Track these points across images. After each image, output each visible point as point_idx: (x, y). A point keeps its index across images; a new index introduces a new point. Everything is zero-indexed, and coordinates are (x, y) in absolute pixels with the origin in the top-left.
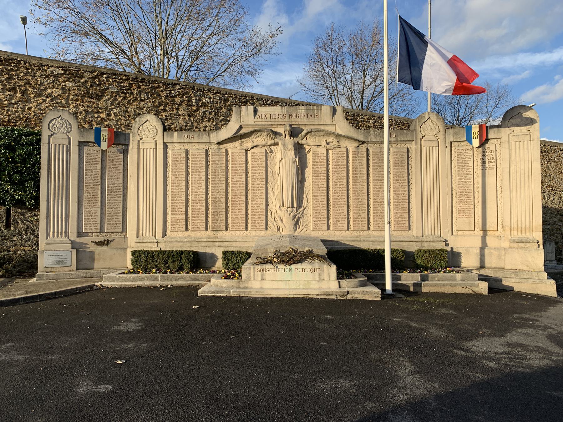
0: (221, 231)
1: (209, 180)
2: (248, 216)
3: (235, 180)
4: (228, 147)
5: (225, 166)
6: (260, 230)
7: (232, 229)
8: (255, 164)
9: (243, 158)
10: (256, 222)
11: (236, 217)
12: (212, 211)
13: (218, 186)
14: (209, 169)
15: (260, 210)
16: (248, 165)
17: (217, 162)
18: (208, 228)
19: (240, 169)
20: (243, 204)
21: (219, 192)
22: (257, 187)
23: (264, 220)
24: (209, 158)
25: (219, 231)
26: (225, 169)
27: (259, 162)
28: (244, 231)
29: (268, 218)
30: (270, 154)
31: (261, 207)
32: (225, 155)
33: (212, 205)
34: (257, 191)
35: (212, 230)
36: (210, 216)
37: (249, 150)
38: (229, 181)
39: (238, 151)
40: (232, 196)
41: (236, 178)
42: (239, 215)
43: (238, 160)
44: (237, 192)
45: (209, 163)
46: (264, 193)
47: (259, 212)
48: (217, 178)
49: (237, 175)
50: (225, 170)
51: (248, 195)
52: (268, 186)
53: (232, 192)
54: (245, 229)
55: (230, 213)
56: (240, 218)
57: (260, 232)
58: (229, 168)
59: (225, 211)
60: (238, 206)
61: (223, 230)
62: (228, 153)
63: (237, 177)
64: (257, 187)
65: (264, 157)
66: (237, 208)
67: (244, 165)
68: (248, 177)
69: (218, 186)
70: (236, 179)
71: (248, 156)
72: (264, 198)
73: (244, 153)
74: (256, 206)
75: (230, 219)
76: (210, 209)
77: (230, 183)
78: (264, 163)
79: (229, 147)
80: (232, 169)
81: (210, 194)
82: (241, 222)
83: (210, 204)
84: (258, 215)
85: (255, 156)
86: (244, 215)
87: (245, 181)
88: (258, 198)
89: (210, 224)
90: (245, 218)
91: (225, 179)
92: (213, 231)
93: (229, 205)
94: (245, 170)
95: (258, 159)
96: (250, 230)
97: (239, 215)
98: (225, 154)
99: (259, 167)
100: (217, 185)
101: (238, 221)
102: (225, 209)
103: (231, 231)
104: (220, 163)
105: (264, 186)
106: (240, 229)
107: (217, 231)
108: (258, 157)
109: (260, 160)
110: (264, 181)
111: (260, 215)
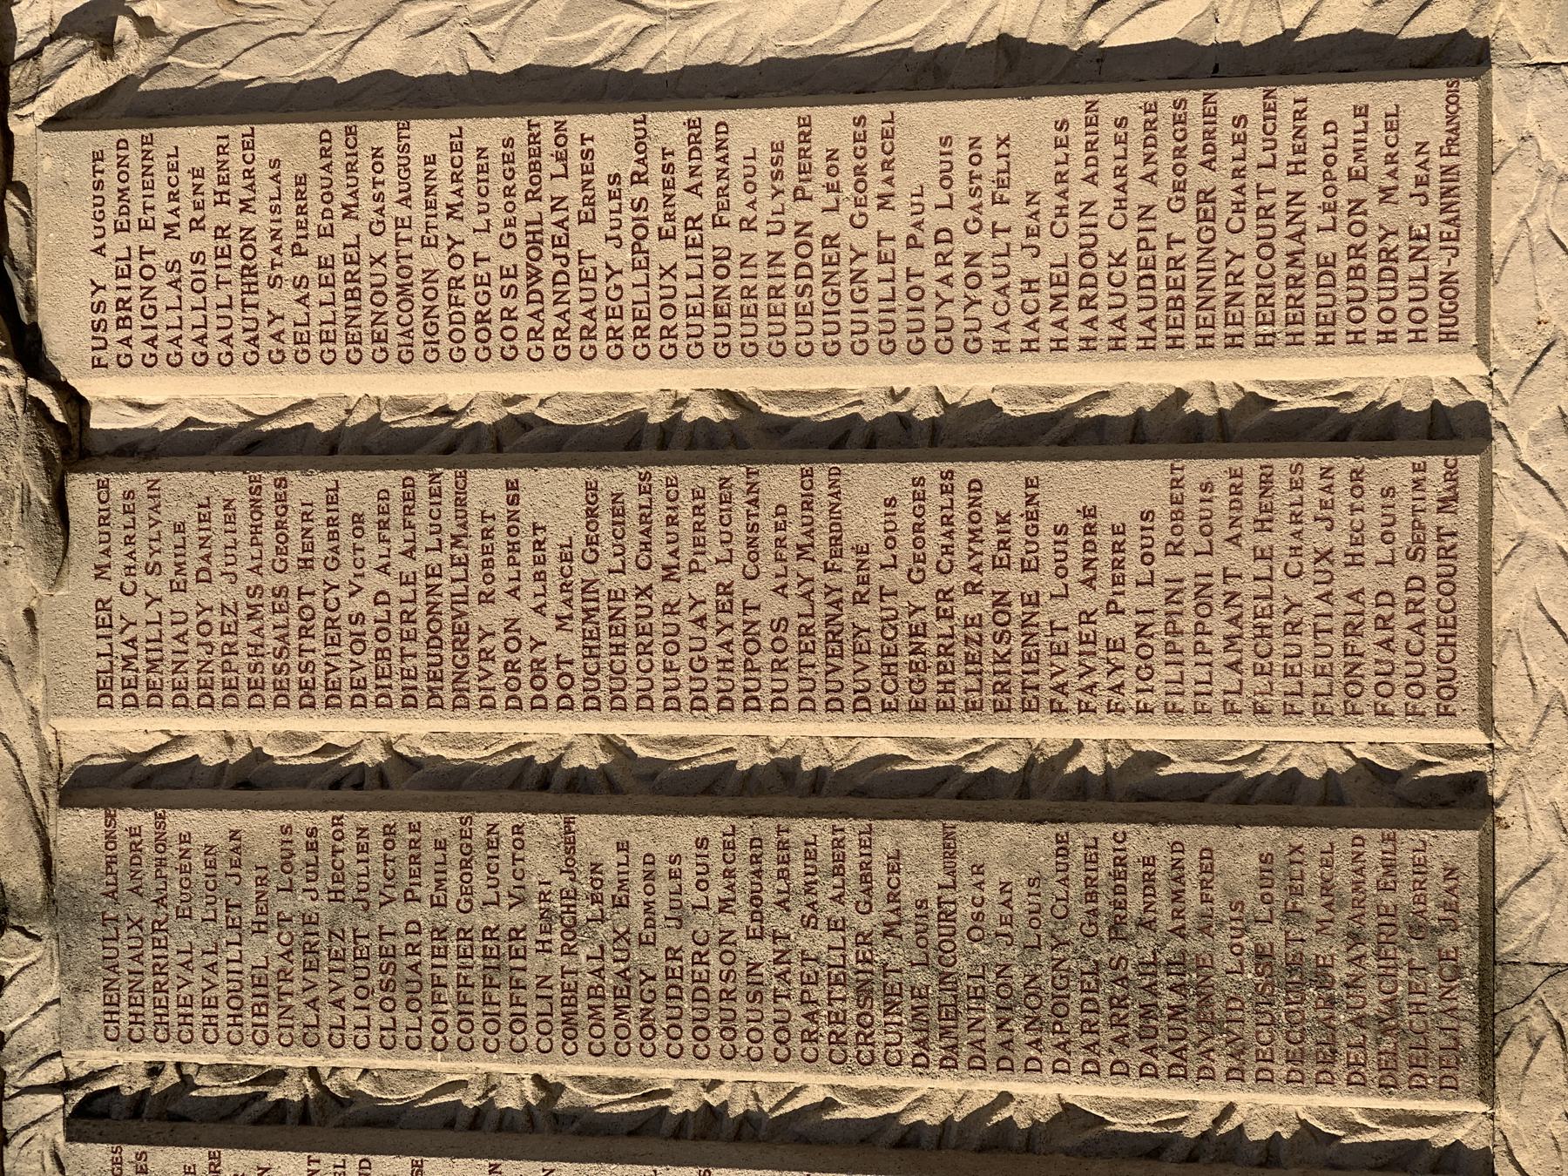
0: (1489, 907)
1: (576, 1096)
2: (1200, 404)
3: (569, 644)
4: (31, 769)
5: (322, 819)
6: (1487, 169)
7: (1466, 703)
8: (282, 300)
9: (186, 512)
10: (1334, 243)
11: (1218, 624)
12: (1121, 1071)
13: (668, 937)
14: (393, 1097)
15: (1103, 196)
16: (324, 421)
17: (259, 951)
18: (1440, 1137)
19: (373, 551)
20: (993, 501)
21: (776, 920)
22: (671, 253)
23: (1286, 96)
24: (210, 1088)
25: (1487, 936)
26: (374, 819)
27: (261, 220)
28: (1504, 469)
29: (1253, 37)
30: (133, 57)
31: (1034, 171)
32: (144, 819)
33: (1005, 1066)
34: (760, 243)
35: (1467, 1077)
36: (1211, 1098)
37: (77, 403)
38: (587, 758)
39: (80, 589)
40: (834, 706)
41: (534, 626)
42: (1185, 567)
43: (237, 594)
44: (774, 608)
45: (289, 1091)
46: (777, 123)
47: (1139, 193)
48: (535, 964)
49: (479, 616)
50: (401, 819)
51: (833, 411)
52: (672, 62)
53: (779, 706)
54: (1469, 465)
55: (1150, 735)
56: (1237, 558)
57: (1512, 180)
58: (372, 755)
59: (1104, 832)
60: (1014, 581)
61: (1470, 878)
62: (133, 760)
63: (505, 608)
64: (671, 253)
65: (168, 138)
66: (1065, 612)
67: (307, 486)
68: (525, 423)
69: (668, 937)
70: (542, 627)
71: (167, 420)
72: (875, 112)
73: (120, 483)
74: (1023, 266)
75: (1252, 733)
76: (1082, 1092)
77: (617, 727)
78: (271, 138)
79: (26, 747)
80: (384, 705)
81: (815, 1086)
82: (1316, 537)
83: (985, 1088)
84: (1186, 225)
85: (165, 296)
86: (1196, 470)
87: (580, 475)
88: (879, 220)
89: (1353, 1104)
90: (1251, 467)
91: (549, 824)
92: (1489, 1050)
93: (1005, 762)
94: (390, 479)
95: (204, 241)
96: (1468, 368)
97: (1185, 567)
98: (127, 818)
99: (346, 231)
100: (654, 960)
101: (1302, 589)
102: (1079, 835)
103: (1487, 722)
104: (284, 905)
105: (668, 126)
106: (1468, 547)
107: (1486, 990)
108: (167, 251)
109: (229, 215)
110: (577, 124)
111: (1198, 179)
